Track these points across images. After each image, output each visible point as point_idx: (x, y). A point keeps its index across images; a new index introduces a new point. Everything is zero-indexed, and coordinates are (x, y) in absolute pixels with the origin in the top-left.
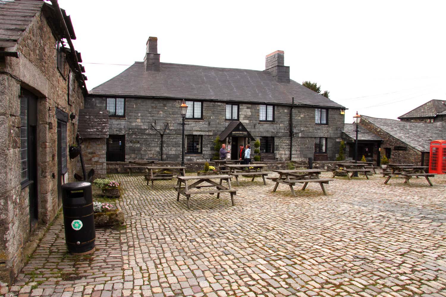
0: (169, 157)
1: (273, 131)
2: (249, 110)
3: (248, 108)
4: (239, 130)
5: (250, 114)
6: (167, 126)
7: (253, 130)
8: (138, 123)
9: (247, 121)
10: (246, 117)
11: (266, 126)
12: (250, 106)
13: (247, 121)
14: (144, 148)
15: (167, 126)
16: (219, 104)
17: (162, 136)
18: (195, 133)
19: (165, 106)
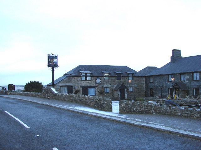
0: (164, 96)
1: (198, 85)
2: (188, 76)
3: (188, 75)
4: (176, 86)
5: (189, 78)
6: (163, 85)
7: (189, 85)
8: (156, 84)
9: (187, 81)
10: (187, 79)
11: (195, 83)
12: (188, 74)
13: (187, 81)
14: (158, 93)
15: (163, 85)
16: (178, 75)
17: (162, 88)
18: (171, 87)
19: (163, 77)
